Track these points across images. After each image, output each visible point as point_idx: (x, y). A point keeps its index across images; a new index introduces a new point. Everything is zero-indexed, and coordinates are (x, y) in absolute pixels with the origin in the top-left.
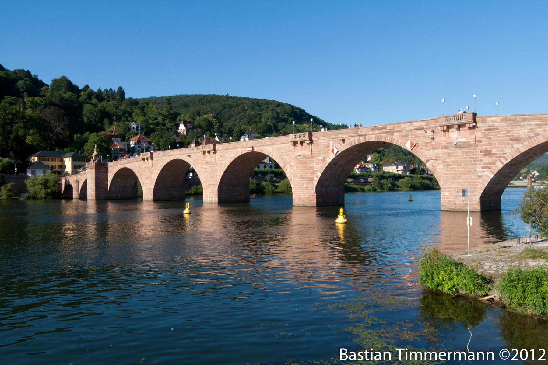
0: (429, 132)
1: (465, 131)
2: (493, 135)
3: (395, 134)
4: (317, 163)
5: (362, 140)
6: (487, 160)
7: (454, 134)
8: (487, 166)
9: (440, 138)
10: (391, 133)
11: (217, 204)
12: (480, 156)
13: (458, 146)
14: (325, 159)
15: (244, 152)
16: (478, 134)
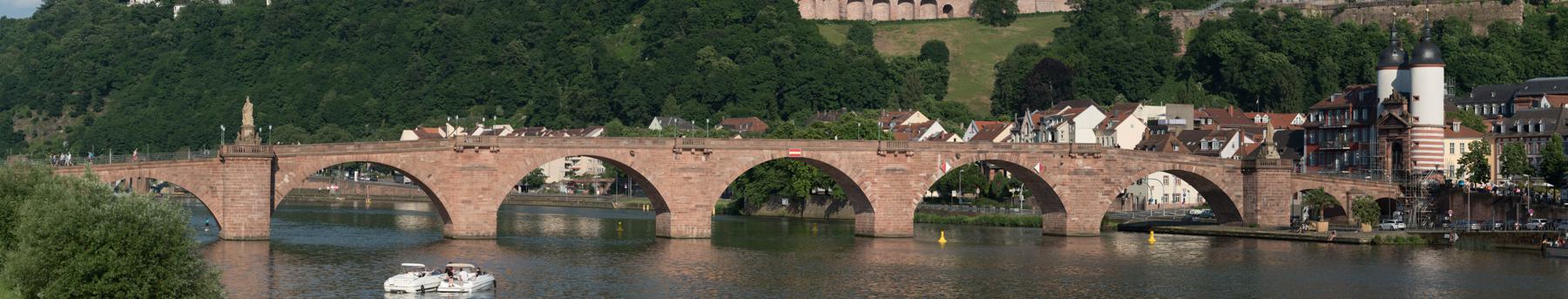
0: (1058, 157)
1: (1090, 160)
2: (1112, 165)
3: (1023, 156)
4: (918, 181)
5: (982, 157)
6: (1107, 188)
7: (1079, 162)
8: (1107, 193)
9: (1068, 164)
10: (1017, 153)
11: (708, 243)
12: (1101, 184)
13: (1089, 173)
14: (928, 177)
15: (777, 157)
16: (1100, 164)
